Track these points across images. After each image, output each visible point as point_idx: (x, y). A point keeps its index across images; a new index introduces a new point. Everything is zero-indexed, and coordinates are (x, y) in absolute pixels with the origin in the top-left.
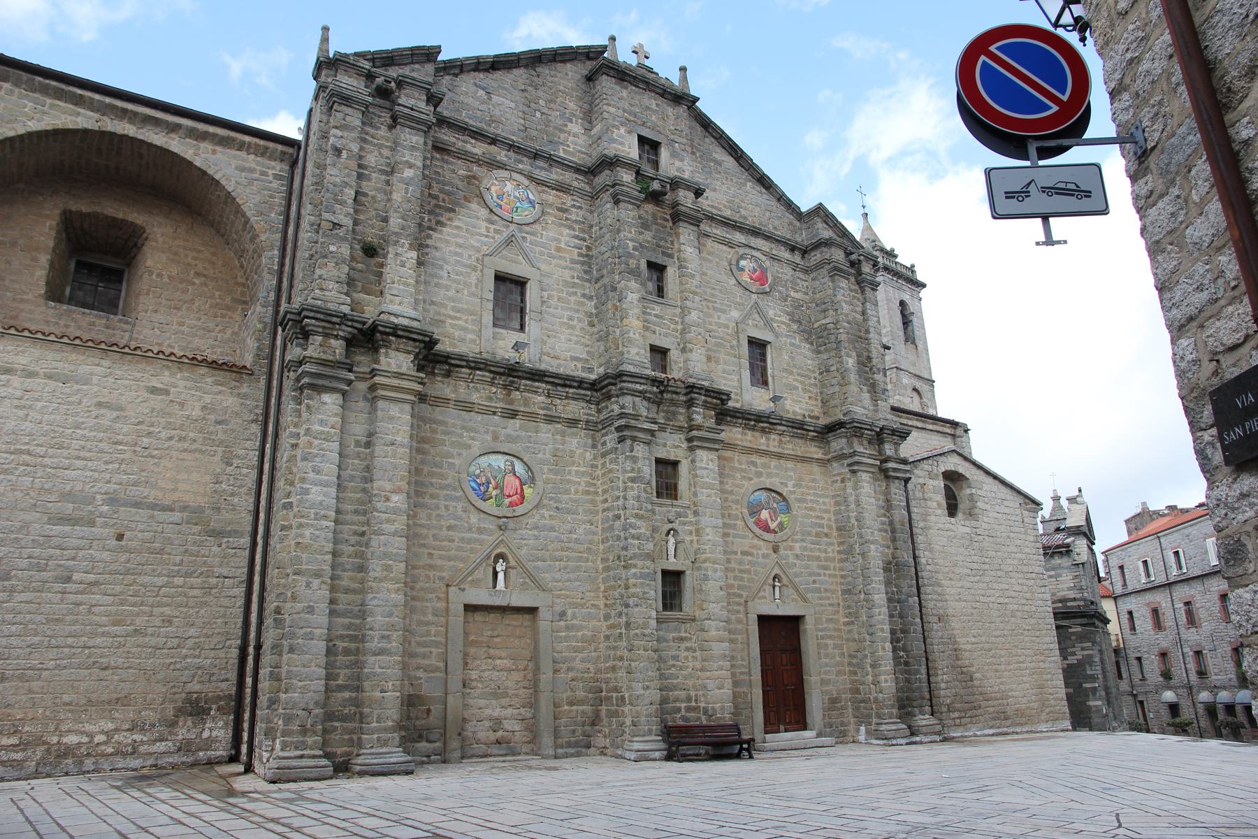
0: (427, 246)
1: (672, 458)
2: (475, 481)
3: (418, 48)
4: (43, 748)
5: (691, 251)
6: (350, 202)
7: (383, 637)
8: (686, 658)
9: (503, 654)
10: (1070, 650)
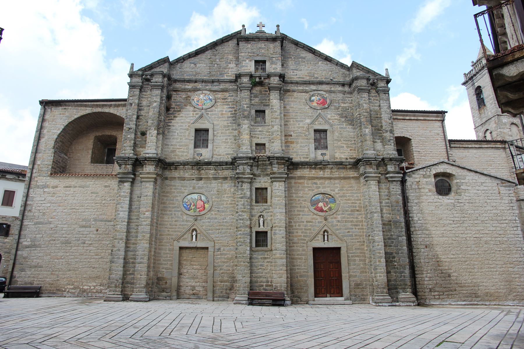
0: (170, 126)
1: (263, 187)
2: (186, 204)
3: (159, 60)
4: (79, 289)
5: (276, 101)
6: (135, 120)
7: (141, 258)
8: (267, 265)
9: (197, 264)
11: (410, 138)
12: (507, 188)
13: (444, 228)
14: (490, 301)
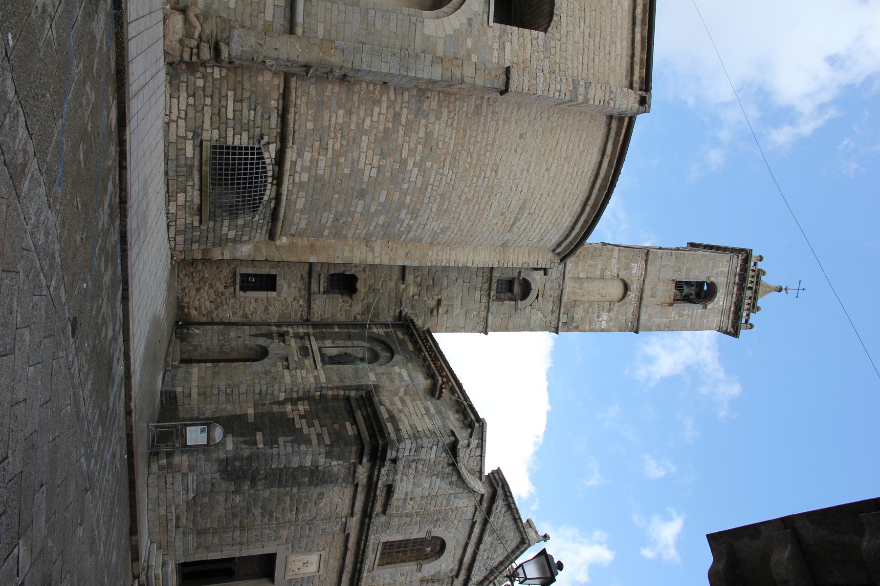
10: (316, 422)
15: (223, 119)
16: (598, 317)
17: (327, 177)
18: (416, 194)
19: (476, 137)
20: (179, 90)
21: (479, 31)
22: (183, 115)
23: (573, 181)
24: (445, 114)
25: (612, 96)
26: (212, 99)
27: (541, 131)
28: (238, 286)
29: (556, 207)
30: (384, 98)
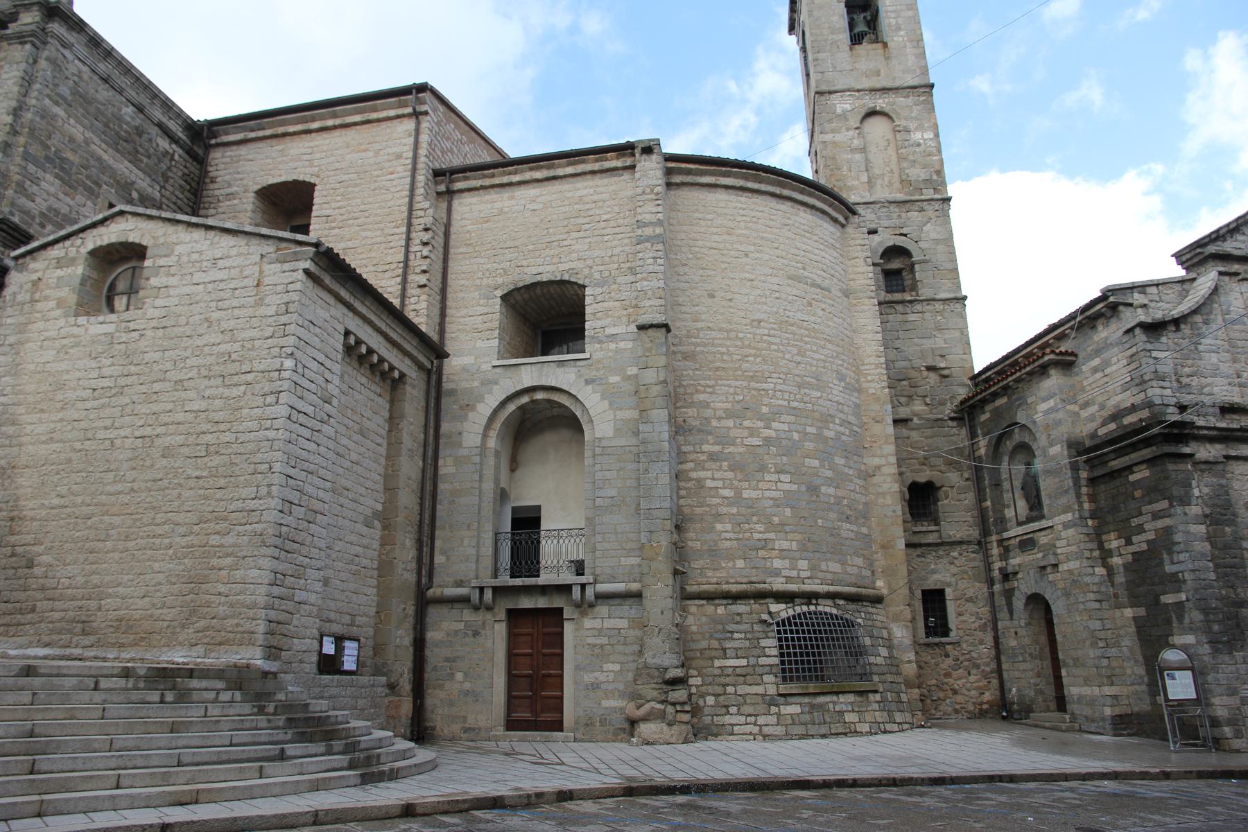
10: (1135, 522)
11: (312, 181)
12: (287, 266)
13: (60, 415)
14: (122, 646)
15: (750, 670)
16: (919, 145)
17: (799, 537)
18: (803, 420)
19: (722, 354)
20: (723, 725)
21: (598, 370)
22: (752, 719)
23: (754, 220)
24: (702, 397)
25: (648, 190)
26: (728, 685)
27: (701, 272)
28: (943, 640)
29: (790, 235)
30: (694, 475)
